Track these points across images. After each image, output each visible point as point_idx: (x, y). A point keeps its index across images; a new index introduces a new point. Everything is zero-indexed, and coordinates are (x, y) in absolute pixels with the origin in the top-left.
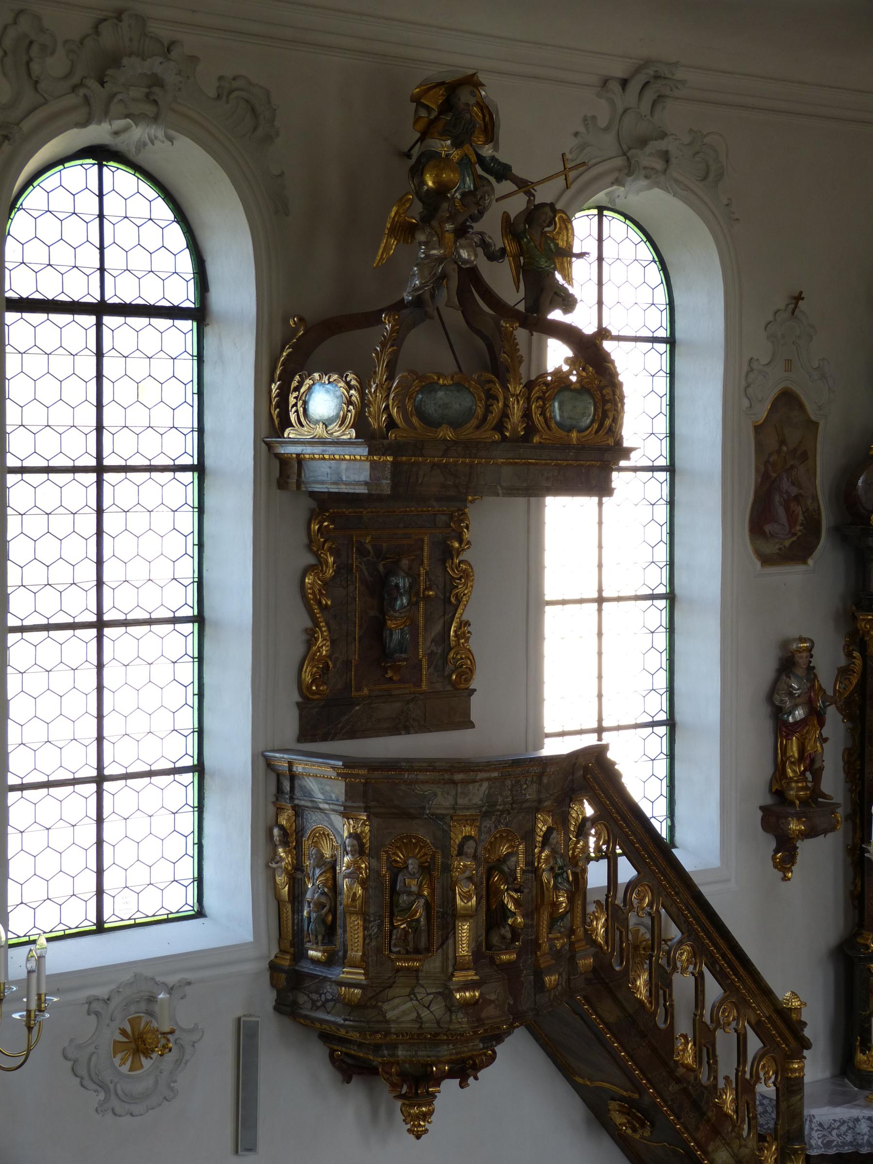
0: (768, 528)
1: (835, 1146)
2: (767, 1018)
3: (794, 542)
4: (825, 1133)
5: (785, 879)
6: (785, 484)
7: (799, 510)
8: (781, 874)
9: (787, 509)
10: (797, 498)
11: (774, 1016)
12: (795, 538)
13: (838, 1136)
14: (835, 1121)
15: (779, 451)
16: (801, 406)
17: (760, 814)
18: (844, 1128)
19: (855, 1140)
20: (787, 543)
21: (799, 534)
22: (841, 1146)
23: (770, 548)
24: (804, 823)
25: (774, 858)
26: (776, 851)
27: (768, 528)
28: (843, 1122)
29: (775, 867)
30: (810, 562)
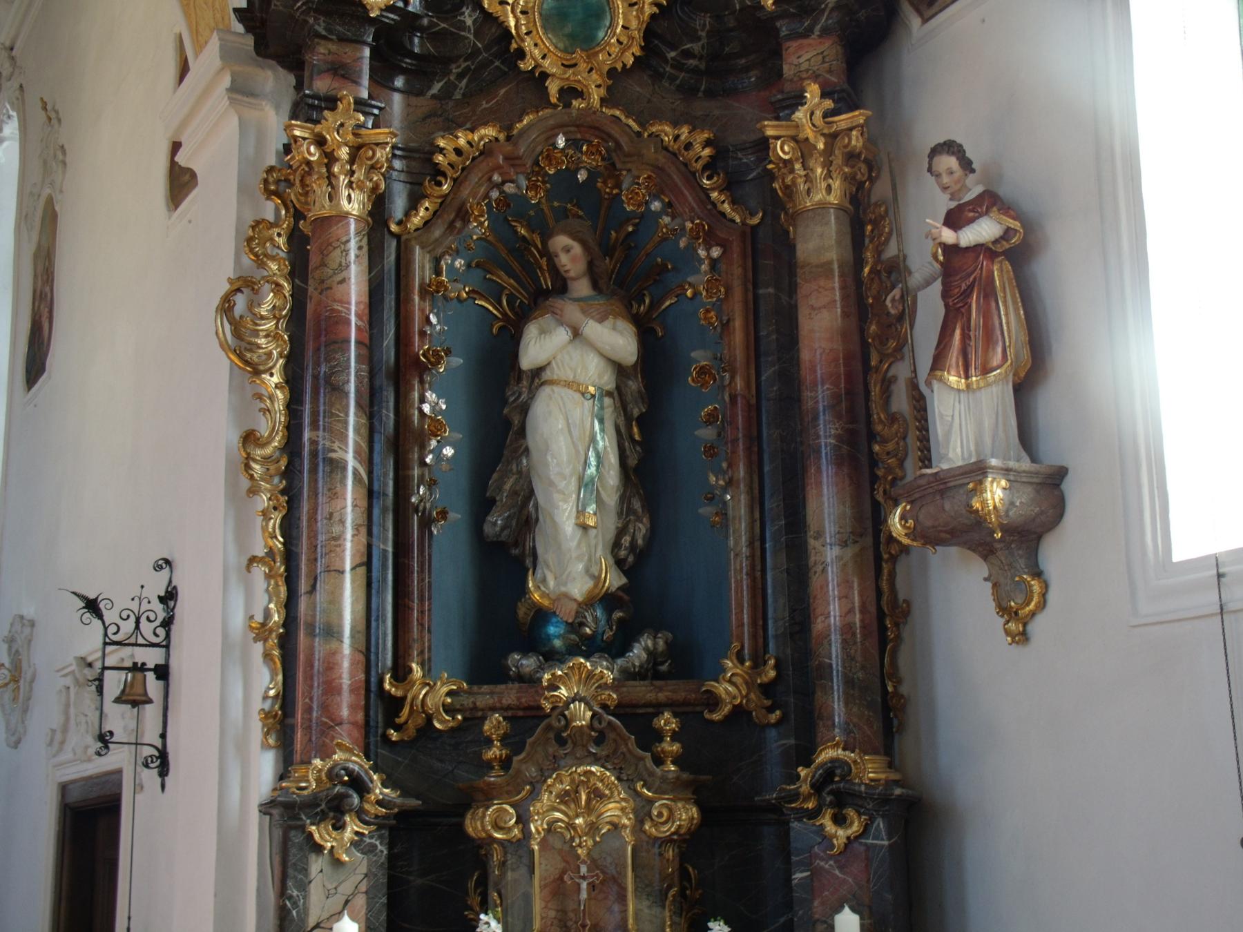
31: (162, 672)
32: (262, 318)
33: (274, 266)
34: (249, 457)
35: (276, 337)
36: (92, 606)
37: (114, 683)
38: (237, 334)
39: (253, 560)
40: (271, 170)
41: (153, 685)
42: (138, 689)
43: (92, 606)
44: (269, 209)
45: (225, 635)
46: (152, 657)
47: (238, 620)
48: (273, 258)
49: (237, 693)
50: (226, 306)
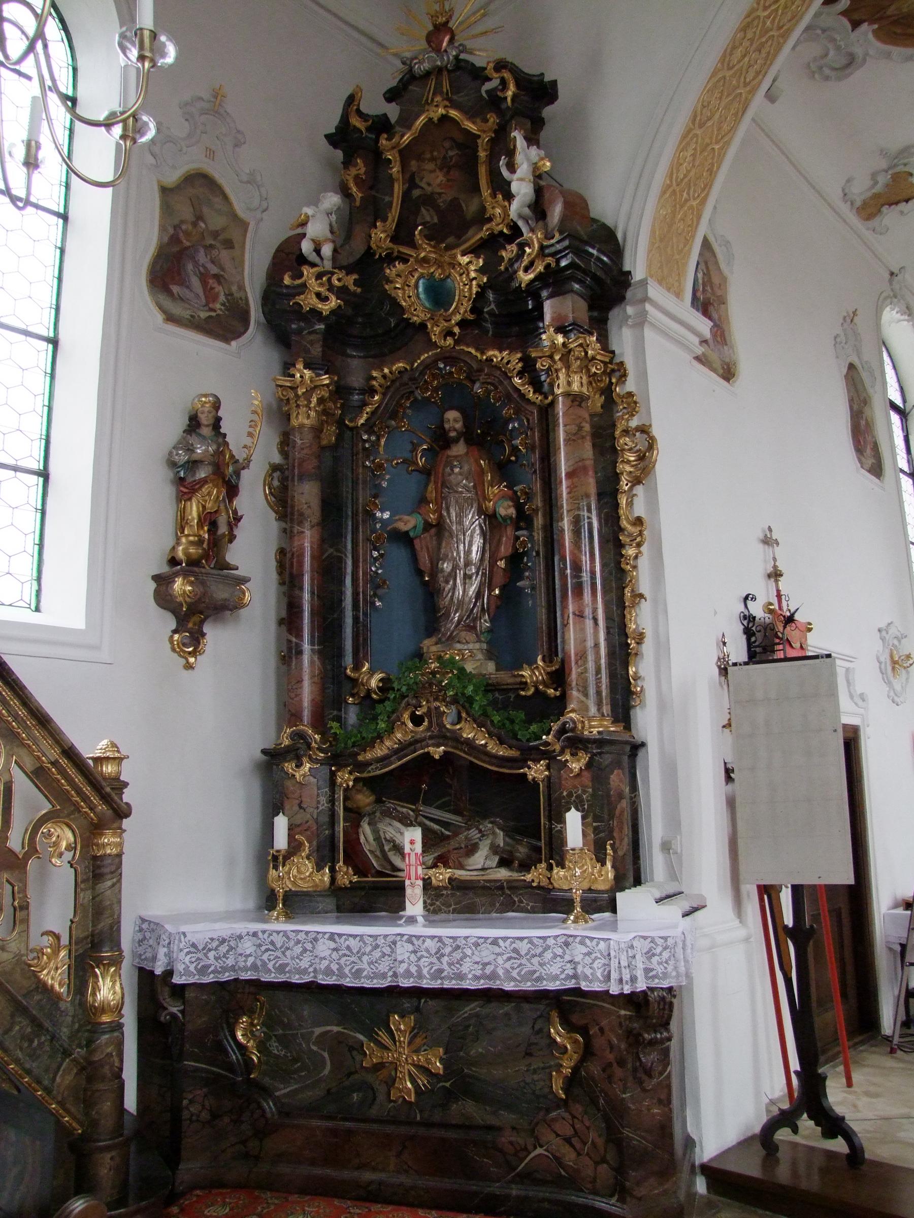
0: (175, 289)
1: (213, 972)
2: (52, 763)
3: (210, 317)
4: (200, 955)
5: (189, 667)
6: (202, 257)
7: (219, 289)
8: (183, 661)
9: (204, 283)
10: (217, 277)
11: (64, 762)
12: (213, 314)
13: (216, 959)
14: (212, 939)
15: (195, 224)
16: (225, 197)
17: (153, 585)
18: (224, 949)
19: (236, 963)
20: (203, 315)
21: (219, 312)
22: (219, 973)
23: (177, 310)
24: (191, 583)
25: (171, 639)
26: (175, 631)
27: (175, 289)
28: (223, 941)
29: (173, 650)
30: (234, 343)
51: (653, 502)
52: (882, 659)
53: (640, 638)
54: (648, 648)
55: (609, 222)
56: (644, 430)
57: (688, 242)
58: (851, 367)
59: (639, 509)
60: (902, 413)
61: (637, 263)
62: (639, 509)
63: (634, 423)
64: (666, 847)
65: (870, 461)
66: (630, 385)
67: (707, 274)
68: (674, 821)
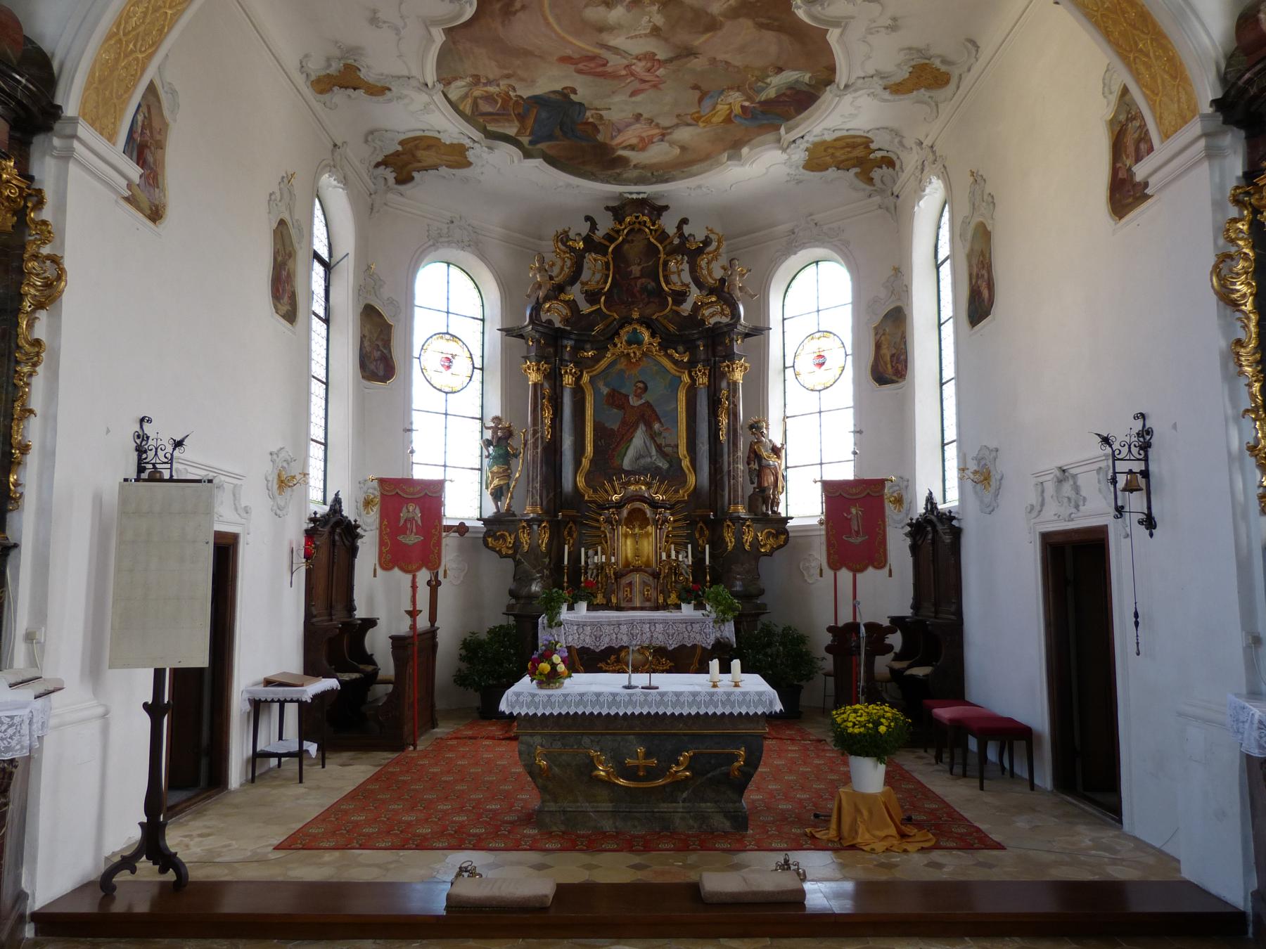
31: (1145, 474)
32: (1238, 274)
33: (1241, 243)
34: (1238, 354)
35: (1249, 284)
36: (1106, 440)
37: (1122, 481)
38: (1224, 286)
39: (1247, 411)
40: (1237, 188)
41: (1142, 482)
42: (1134, 483)
43: (1106, 440)
44: (1233, 212)
45: (1229, 453)
46: (1138, 467)
47: (1235, 444)
48: (1241, 239)
49: (1239, 485)
50: (1216, 270)
51: (55, 329)
52: (270, 478)
53: (25, 449)
54: (32, 461)
55: (46, 46)
56: (55, 260)
57: (129, 90)
58: (282, 223)
59: (40, 331)
60: (327, 267)
61: (71, 99)
62: (40, 331)
63: (46, 250)
64: (30, 637)
65: (285, 308)
66: (46, 214)
67: (148, 118)
68: (40, 613)
